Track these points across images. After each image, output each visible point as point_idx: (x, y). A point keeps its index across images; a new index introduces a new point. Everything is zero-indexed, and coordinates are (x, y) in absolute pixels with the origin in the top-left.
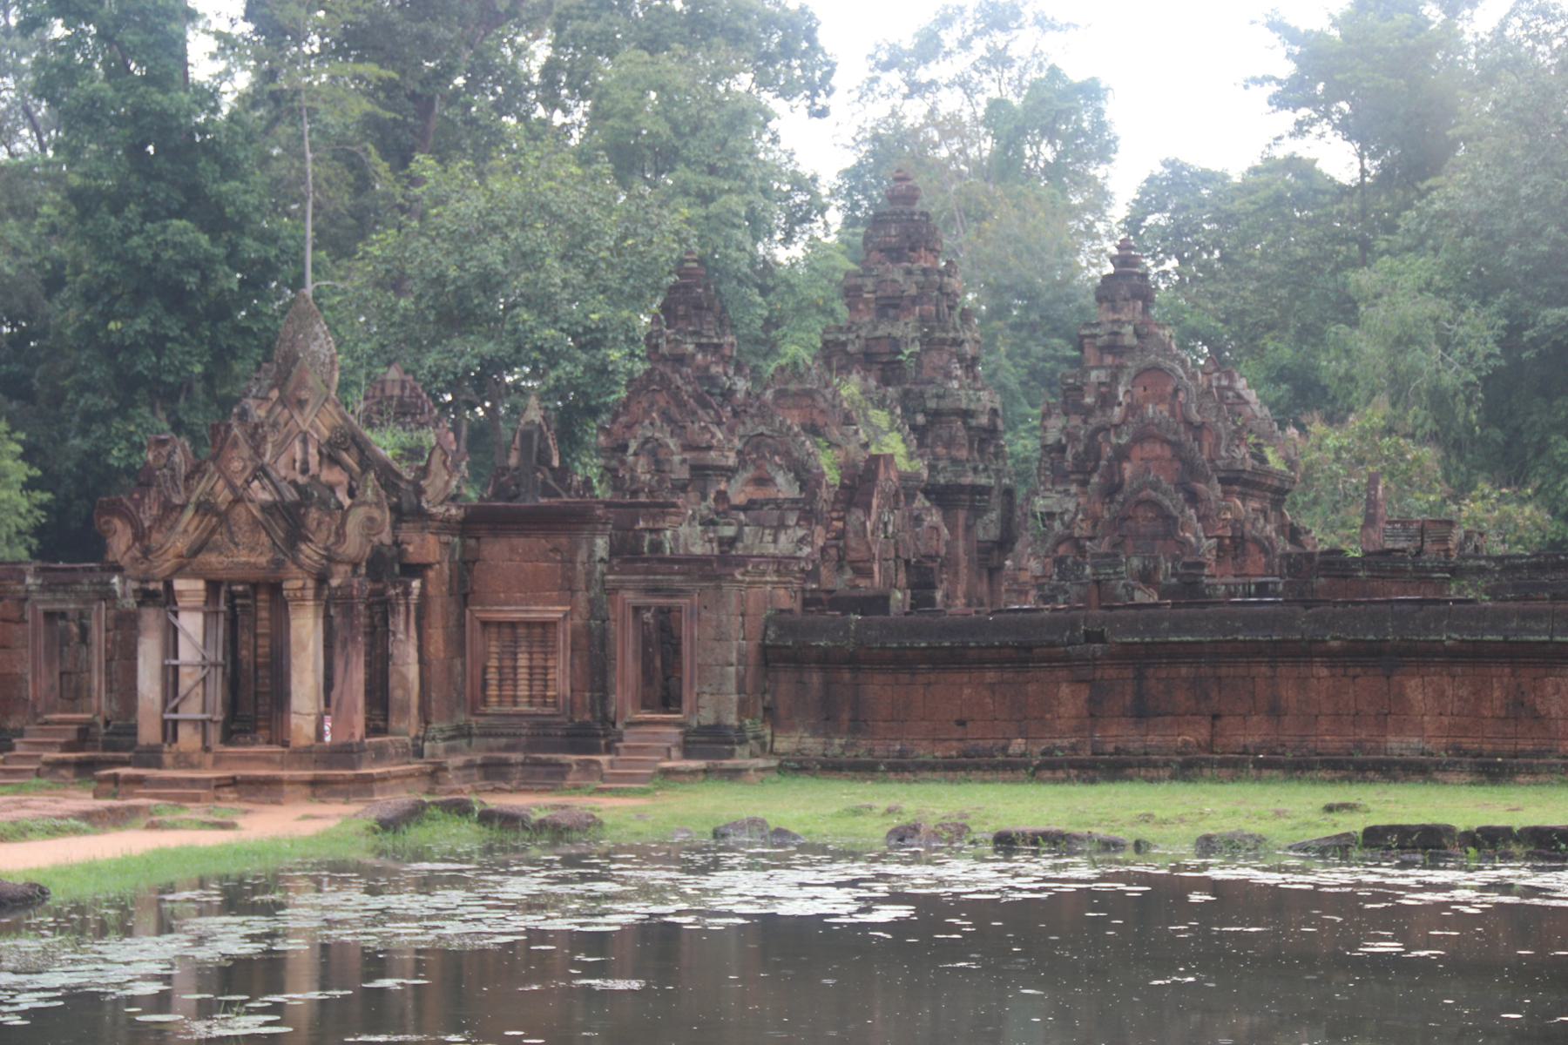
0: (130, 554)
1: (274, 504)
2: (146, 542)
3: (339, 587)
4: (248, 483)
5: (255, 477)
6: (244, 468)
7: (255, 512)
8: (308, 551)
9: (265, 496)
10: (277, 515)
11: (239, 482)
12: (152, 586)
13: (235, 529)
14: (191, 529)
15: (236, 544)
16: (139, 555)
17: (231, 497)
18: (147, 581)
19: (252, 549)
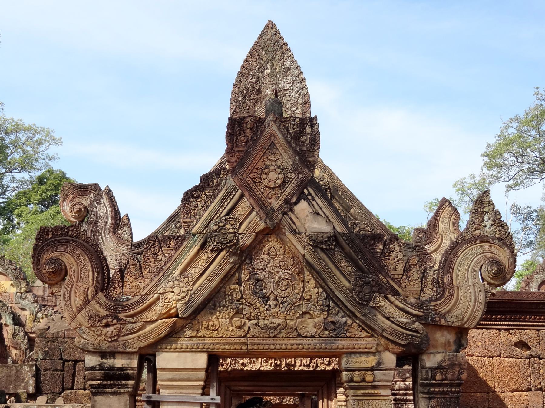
0: (86, 309)
1: (335, 237)
2: (115, 293)
3: (440, 367)
4: (289, 204)
5: (301, 196)
6: (285, 182)
7: (300, 248)
8: (390, 310)
9: (320, 227)
10: (338, 254)
11: (275, 204)
12: (119, 362)
13: (262, 275)
14: (193, 272)
15: (265, 299)
16: (103, 312)
17: (262, 225)
18: (113, 354)
19: (292, 306)
